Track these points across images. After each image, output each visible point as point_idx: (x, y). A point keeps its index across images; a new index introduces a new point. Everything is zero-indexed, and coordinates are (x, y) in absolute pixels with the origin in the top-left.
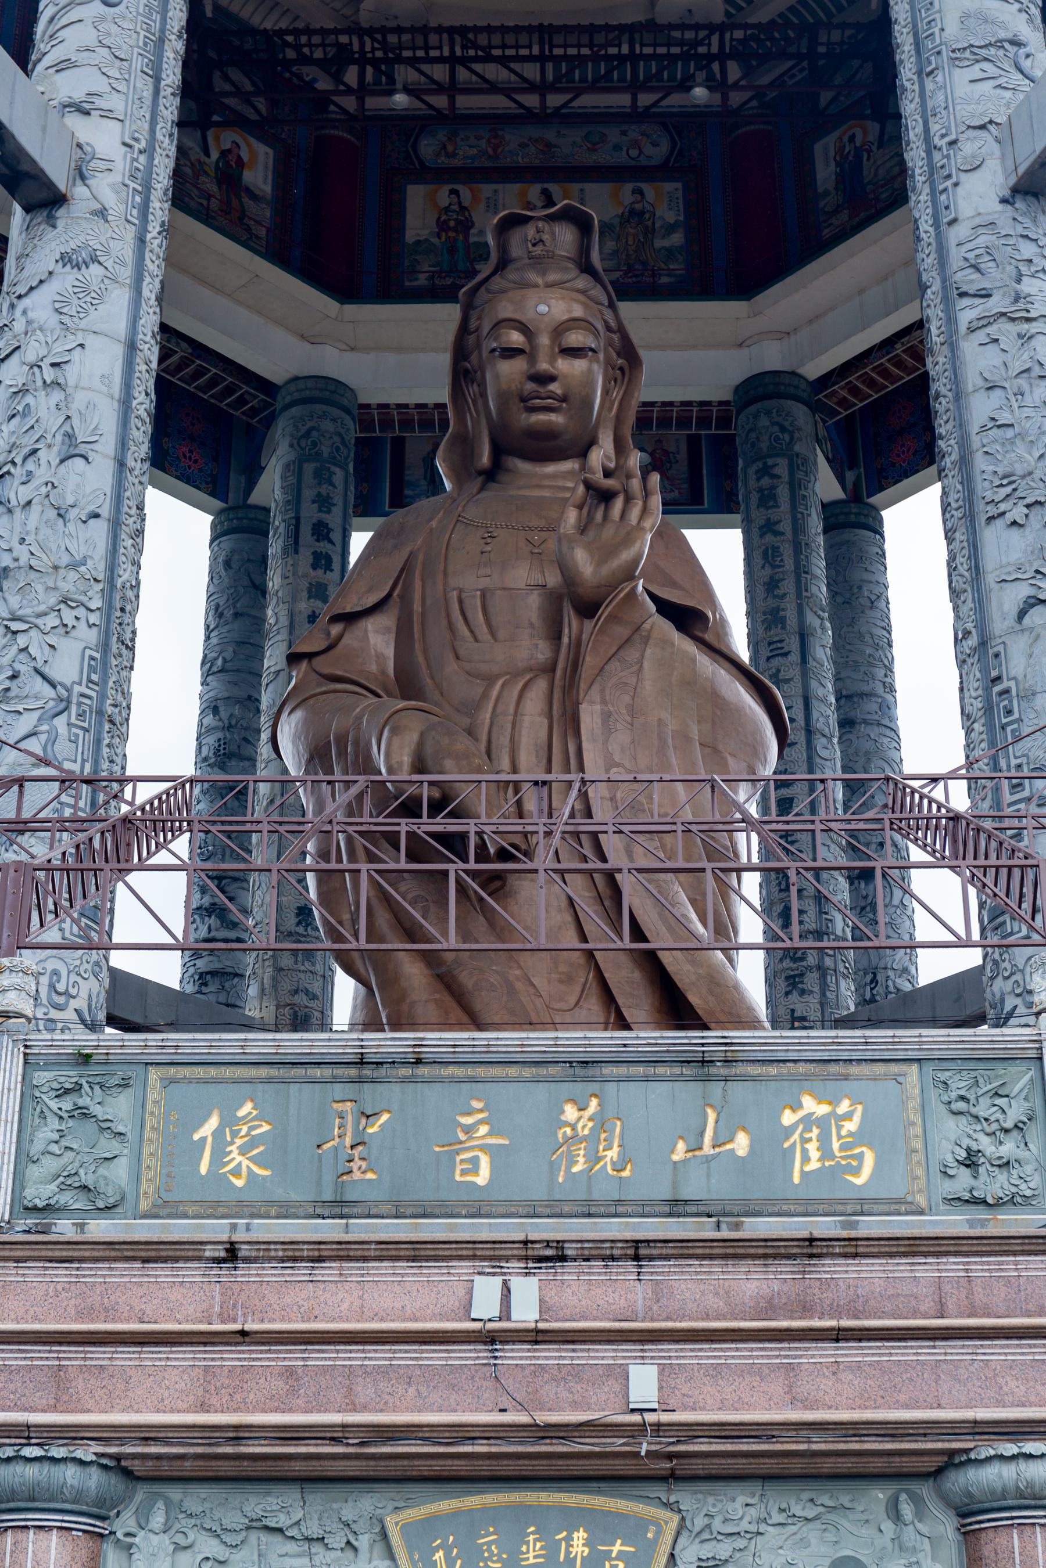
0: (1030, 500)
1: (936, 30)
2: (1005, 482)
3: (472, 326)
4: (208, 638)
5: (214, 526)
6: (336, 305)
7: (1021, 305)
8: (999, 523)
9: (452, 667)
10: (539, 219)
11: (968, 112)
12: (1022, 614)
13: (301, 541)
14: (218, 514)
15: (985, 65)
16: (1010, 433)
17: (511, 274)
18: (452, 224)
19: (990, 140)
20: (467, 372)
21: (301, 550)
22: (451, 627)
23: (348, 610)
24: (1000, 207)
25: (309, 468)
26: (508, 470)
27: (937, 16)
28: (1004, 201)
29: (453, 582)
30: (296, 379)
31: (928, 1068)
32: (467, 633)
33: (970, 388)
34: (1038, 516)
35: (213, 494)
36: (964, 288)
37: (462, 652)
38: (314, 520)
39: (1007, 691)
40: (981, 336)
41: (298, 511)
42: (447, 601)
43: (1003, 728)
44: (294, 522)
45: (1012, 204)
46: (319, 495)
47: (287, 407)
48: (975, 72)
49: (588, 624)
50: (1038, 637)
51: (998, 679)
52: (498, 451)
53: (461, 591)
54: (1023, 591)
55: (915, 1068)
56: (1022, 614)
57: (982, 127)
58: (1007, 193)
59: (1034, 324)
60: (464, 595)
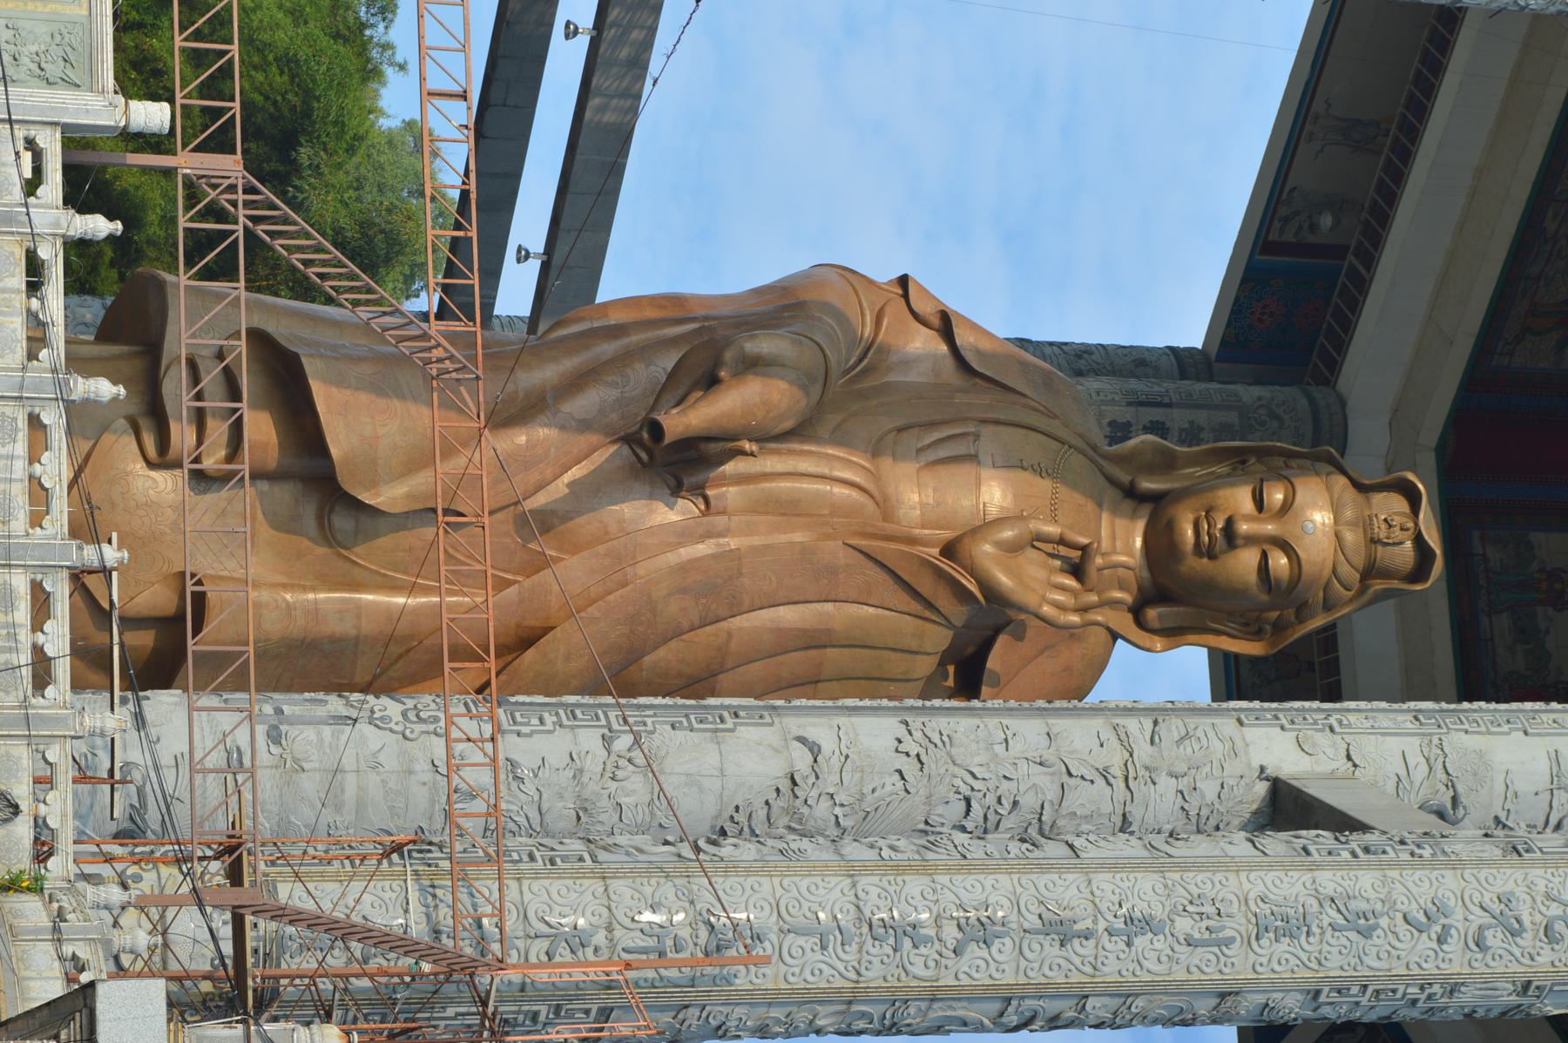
0: (924, 758)
1: (1466, 726)
2: (945, 738)
3: (1294, 463)
4: (1051, 344)
5: (1191, 351)
6: (1434, 445)
7: (1142, 772)
8: (901, 731)
9: (888, 424)
10: (1416, 524)
11: (1366, 748)
12: (802, 740)
13: (1142, 409)
14: (1202, 353)
15: (1424, 768)
16: (1000, 749)
17: (1350, 494)
18: (1558, 586)
19: (1334, 765)
20: (1244, 462)
21: (1133, 409)
22: (933, 425)
23: (955, 330)
24: (1256, 764)
25: (1232, 417)
26: (1135, 510)
27: (1483, 729)
28: (1262, 769)
29: (986, 431)
30: (1343, 403)
31: (86, 21)
32: (927, 441)
33: (1051, 721)
34: (910, 768)
35: (1224, 343)
36: (1161, 725)
37: (905, 434)
38: (1168, 424)
39: (722, 720)
40: (1108, 734)
41: (1179, 405)
42: (965, 420)
43: (687, 716)
44: (1166, 400)
45: (1260, 778)
46: (1200, 429)
47: (1312, 401)
48: (1415, 759)
49: (935, 551)
50: (777, 751)
51: (736, 715)
52: (1156, 500)
53: (977, 436)
54: (827, 744)
55: (85, 13)
56: (802, 740)
57: (1349, 758)
58: (1269, 772)
59: (1123, 785)
60: (971, 438)
